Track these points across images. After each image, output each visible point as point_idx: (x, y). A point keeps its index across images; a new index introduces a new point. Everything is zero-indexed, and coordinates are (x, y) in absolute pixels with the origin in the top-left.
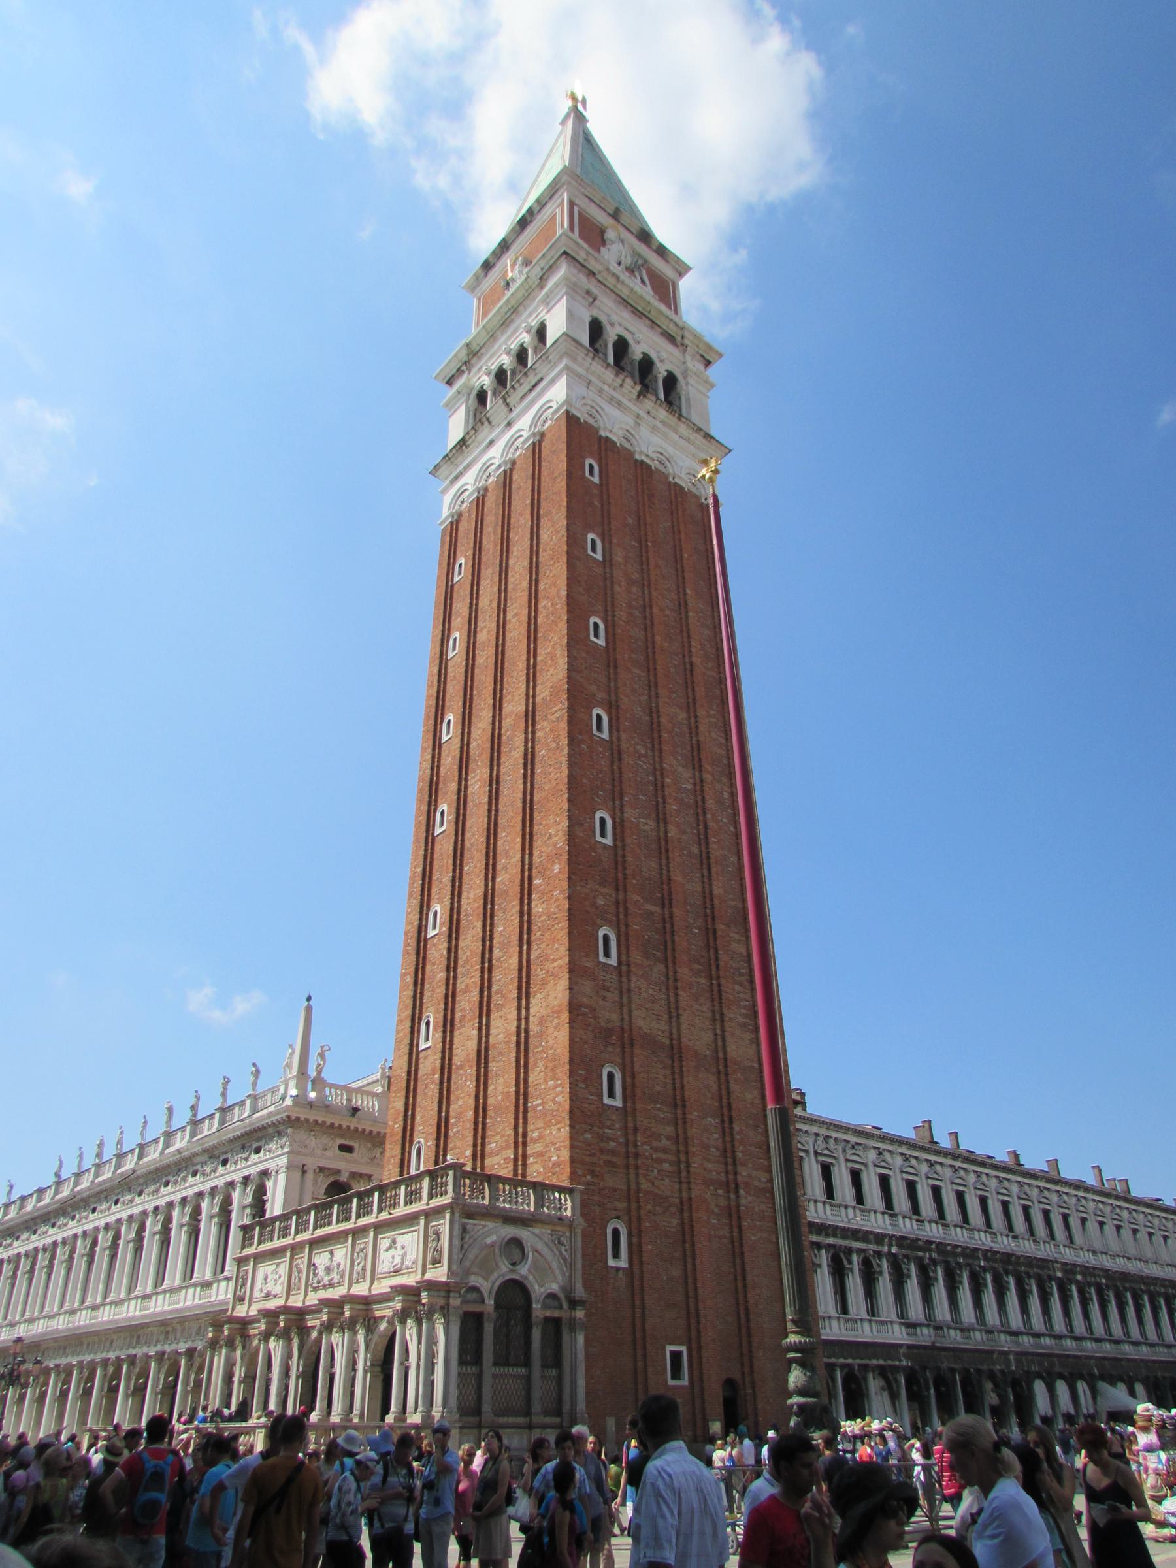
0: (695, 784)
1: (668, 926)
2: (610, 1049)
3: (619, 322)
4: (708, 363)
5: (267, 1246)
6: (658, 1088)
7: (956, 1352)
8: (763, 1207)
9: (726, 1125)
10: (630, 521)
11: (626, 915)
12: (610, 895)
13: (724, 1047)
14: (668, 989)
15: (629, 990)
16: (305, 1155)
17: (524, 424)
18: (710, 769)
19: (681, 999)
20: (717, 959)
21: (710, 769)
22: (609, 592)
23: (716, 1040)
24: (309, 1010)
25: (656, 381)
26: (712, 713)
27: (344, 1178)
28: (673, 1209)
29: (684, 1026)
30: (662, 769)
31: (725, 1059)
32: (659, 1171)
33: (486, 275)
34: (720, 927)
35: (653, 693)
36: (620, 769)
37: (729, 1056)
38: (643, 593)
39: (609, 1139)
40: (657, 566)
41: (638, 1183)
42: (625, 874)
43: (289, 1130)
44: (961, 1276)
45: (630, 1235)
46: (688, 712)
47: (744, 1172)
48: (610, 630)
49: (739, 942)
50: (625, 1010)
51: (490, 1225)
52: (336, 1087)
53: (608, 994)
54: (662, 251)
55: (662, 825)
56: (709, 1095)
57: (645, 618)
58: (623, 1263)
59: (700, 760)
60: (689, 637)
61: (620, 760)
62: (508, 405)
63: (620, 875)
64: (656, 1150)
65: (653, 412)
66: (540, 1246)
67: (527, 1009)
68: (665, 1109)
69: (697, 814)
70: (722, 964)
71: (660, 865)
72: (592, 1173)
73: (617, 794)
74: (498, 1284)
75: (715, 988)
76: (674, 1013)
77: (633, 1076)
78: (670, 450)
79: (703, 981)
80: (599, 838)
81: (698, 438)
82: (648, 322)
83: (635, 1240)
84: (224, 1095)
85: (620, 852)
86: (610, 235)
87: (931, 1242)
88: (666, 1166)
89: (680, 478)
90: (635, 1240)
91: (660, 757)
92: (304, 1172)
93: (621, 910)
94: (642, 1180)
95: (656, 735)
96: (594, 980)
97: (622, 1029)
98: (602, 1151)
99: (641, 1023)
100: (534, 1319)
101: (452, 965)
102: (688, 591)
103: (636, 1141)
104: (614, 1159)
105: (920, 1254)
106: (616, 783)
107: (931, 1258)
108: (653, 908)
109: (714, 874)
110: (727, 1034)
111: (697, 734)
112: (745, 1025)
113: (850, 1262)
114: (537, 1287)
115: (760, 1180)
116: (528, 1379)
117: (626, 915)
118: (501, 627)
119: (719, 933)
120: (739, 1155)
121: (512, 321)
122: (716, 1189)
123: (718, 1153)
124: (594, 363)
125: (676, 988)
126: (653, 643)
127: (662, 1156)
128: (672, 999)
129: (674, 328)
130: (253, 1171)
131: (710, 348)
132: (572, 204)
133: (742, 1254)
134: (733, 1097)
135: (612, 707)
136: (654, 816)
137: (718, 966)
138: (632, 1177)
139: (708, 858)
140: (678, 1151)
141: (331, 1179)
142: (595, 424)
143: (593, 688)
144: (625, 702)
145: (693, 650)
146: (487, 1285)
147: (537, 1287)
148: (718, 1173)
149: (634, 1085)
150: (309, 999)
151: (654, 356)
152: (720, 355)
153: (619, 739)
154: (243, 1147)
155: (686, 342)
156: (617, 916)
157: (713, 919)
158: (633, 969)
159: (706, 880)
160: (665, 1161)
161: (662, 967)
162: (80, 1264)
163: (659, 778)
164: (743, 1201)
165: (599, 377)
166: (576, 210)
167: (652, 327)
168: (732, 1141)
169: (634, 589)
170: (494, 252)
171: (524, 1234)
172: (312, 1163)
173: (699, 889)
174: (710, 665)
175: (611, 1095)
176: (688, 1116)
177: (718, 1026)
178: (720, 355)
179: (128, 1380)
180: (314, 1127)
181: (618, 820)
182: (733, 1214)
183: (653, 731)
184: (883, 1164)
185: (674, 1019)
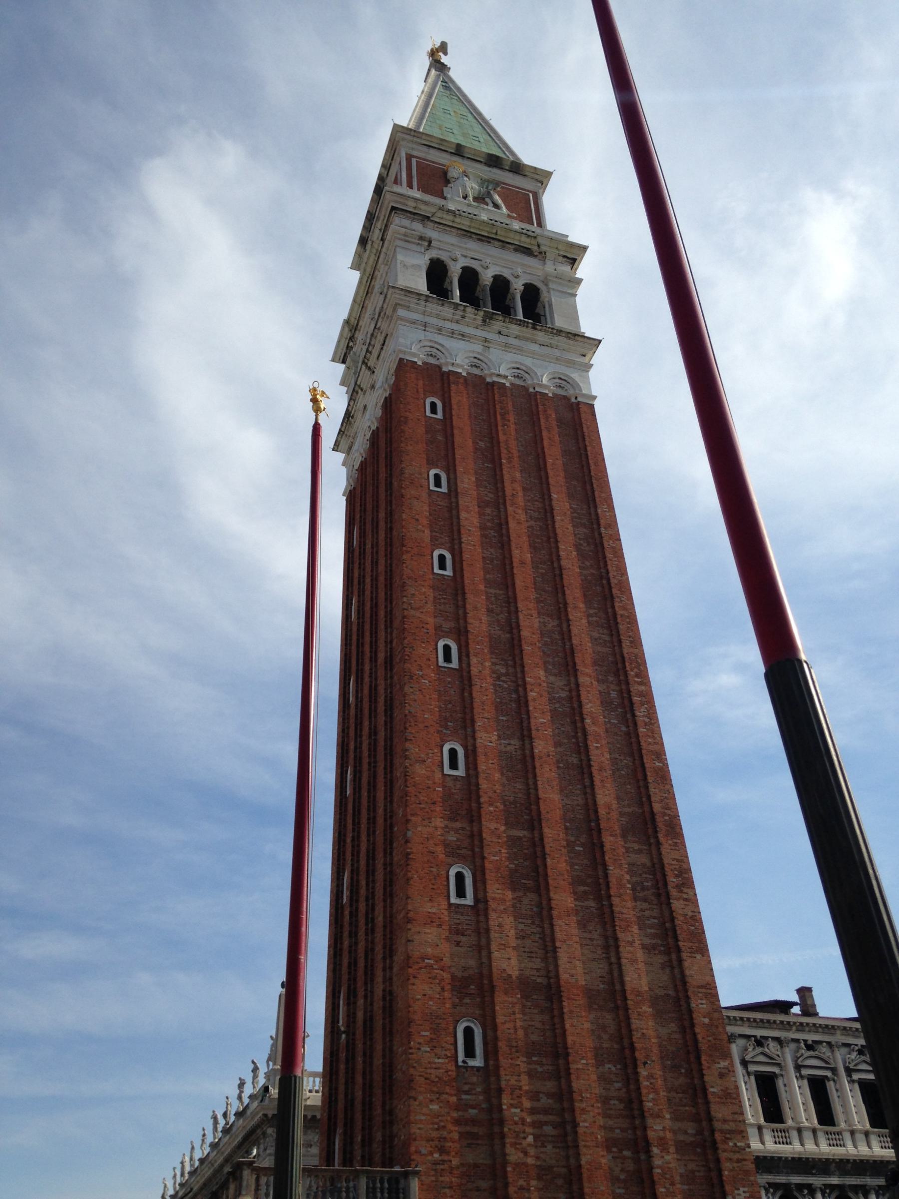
0: (570, 691)
1: (539, 849)
2: (467, 1000)
4: (573, 262)
8: (692, 1166)
10: (482, 444)
12: (463, 829)
13: (621, 975)
14: (542, 921)
15: (488, 930)
18: (587, 671)
19: (557, 929)
22: (455, 520)
23: (611, 972)
28: (560, 1182)
31: (624, 991)
32: (536, 1138)
37: (628, 987)
38: (500, 511)
40: (513, 481)
41: (505, 1155)
42: (479, 803)
46: (559, 618)
49: (639, 852)
54: (517, 168)
55: (527, 742)
56: (605, 1037)
57: (501, 536)
62: (369, 368)
65: (504, 331)
68: (544, 1060)
71: (528, 784)
72: (442, 1150)
73: (468, 722)
75: (607, 910)
77: (495, 1028)
78: (528, 362)
79: (592, 903)
80: (447, 770)
82: (497, 243)
85: (473, 781)
86: (453, 173)
93: (477, 842)
94: (509, 1150)
96: (440, 926)
97: (481, 974)
99: (504, 965)
102: (554, 496)
103: (501, 1105)
104: (475, 1130)
106: (467, 711)
108: (520, 833)
110: (624, 961)
112: (654, 947)
115: (686, 1133)
122: (621, 1151)
123: (622, 1106)
124: (428, 304)
125: (551, 918)
128: (548, 932)
129: (528, 240)
131: (572, 245)
132: (409, 158)
135: (461, 634)
136: (519, 734)
137: (608, 883)
139: (590, 766)
140: (563, 1109)
142: (437, 363)
145: (561, 553)
148: (622, 1130)
151: (506, 274)
152: (584, 249)
153: (469, 665)
155: (543, 248)
156: (473, 850)
157: (599, 831)
158: (492, 905)
159: (588, 790)
160: (546, 1123)
161: (532, 896)
164: (657, 1162)
165: (438, 316)
166: (414, 161)
167: (503, 248)
169: (488, 511)
173: (581, 802)
174: (588, 564)
176: (573, 1066)
177: (613, 954)
178: (584, 249)
181: (470, 748)
183: (511, 649)
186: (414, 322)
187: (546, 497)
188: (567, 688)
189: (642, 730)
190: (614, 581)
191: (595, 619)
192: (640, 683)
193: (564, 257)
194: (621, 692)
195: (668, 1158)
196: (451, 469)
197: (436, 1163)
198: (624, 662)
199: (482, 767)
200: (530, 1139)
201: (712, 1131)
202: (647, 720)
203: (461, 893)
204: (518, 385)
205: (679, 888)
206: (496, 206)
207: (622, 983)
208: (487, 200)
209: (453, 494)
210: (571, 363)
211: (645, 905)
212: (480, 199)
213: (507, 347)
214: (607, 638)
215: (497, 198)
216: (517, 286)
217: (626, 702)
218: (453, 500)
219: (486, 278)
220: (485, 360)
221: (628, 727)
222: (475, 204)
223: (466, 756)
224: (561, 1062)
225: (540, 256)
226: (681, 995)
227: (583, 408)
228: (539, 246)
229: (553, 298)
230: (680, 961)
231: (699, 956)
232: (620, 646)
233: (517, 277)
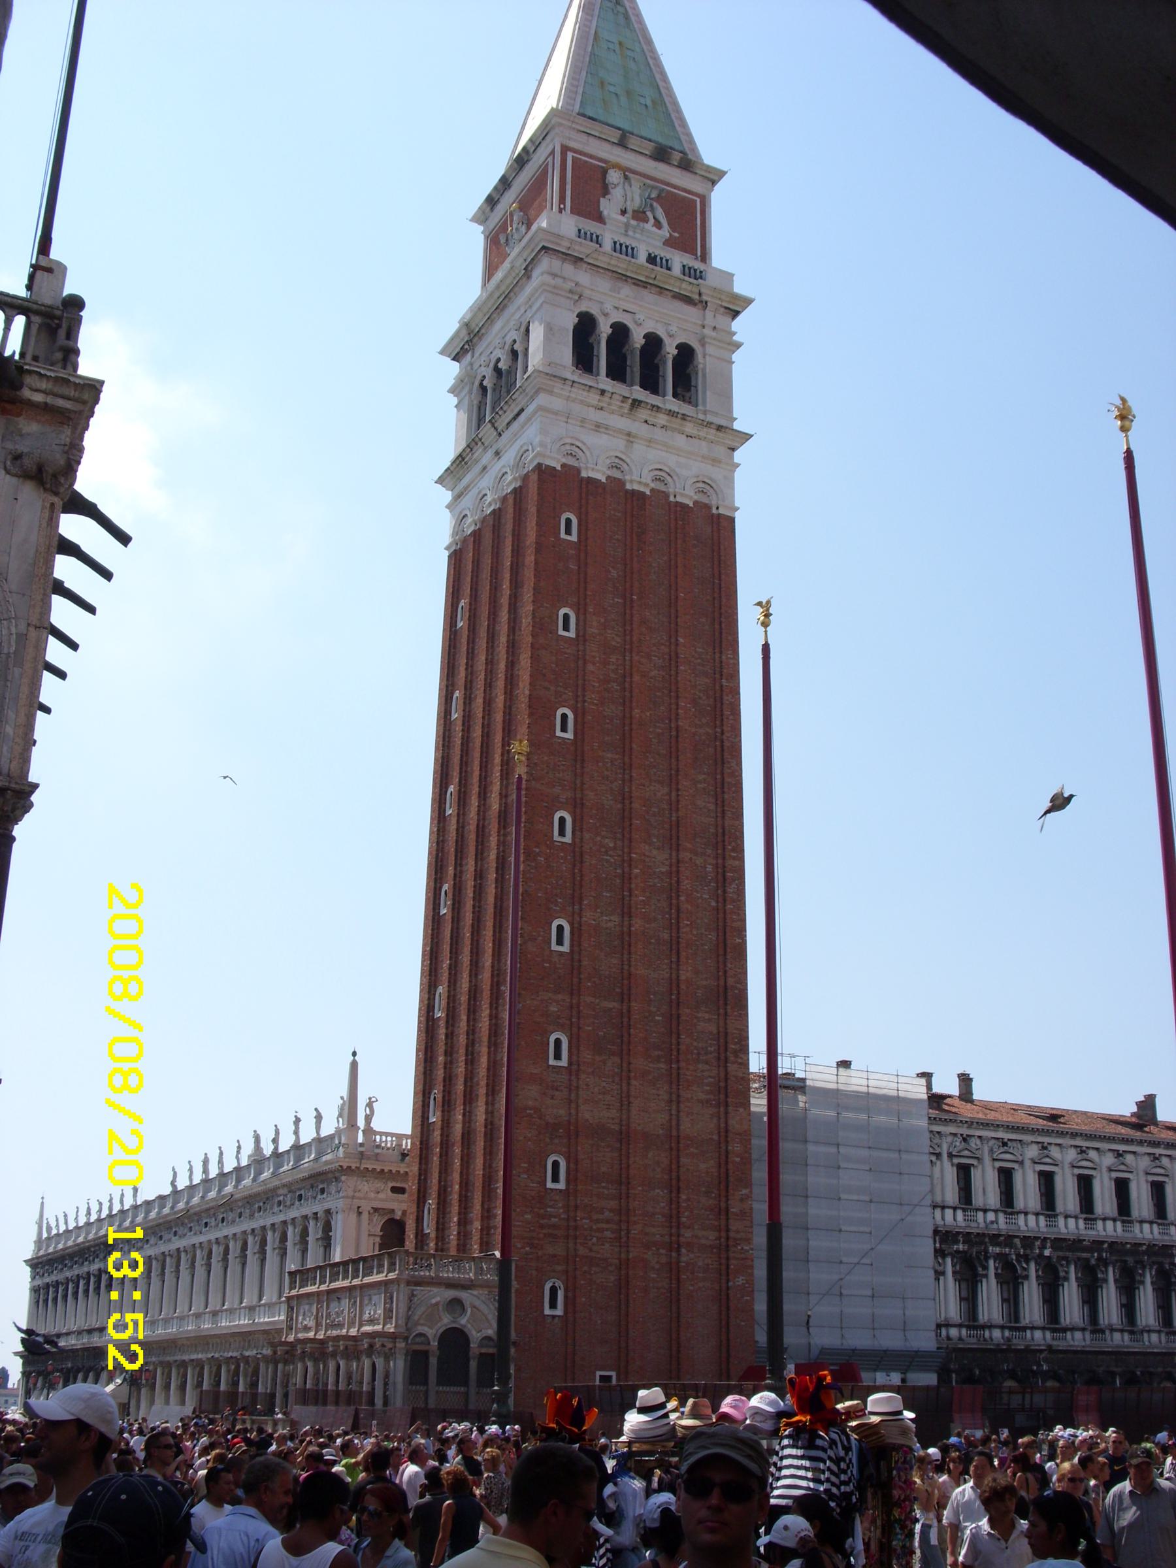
0: (671, 866)
1: (625, 1020)
2: (556, 1141)
4: (736, 314)
5: (304, 1291)
6: (604, 1169)
7: (1118, 1355)
9: (674, 1195)
11: (579, 1018)
13: (678, 1125)
15: (577, 1088)
16: (360, 1199)
17: (509, 457)
18: (688, 845)
19: (632, 1088)
20: (678, 1044)
21: (688, 845)
23: (670, 1120)
24: (354, 1066)
25: (665, 363)
26: (702, 777)
27: (398, 1215)
29: (634, 1112)
30: (631, 859)
32: (598, 1239)
33: (492, 209)
34: (685, 1011)
35: (627, 777)
36: (581, 871)
39: (551, 1216)
43: (343, 1178)
44: (1143, 1275)
45: (566, 1290)
47: (688, 1234)
48: (579, 720)
49: (710, 1020)
50: (573, 1105)
51: (435, 1290)
52: (387, 1134)
53: (557, 1093)
54: (688, 163)
57: (624, 689)
58: (559, 1312)
59: (678, 837)
60: (677, 697)
61: (582, 862)
62: (496, 429)
63: (575, 980)
64: (598, 1221)
65: (651, 420)
66: (477, 1303)
67: (493, 1104)
69: (671, 898)
70: (682, 1047)
74: (441, 1331)
75: (674, 1072)
76: (625, 1101)
77: (577, 1162)
79: (662, 1065)
80: (554, 947)
82: (654, 289)
83: (570, 1294)
84: (296, 1133)
85: (576, 957)
86: (614, 176)
87: (1103, 1242)
88: (608, 1234)
89: (682, 495)
90: (570, 1294)
91: (630, 847)
92: (360, 1213)
95: (627, 824)
97: (569, 1122)
98: (542, 1227)
99: (587, 1116)
100: (471, 1354)
101: (449, 1052)
102: (681, 640)
104: (556, 1232)
105: (1085, 1255)
107: (1100, 1259)
108: (610, 1005)
109: (683, 959)
111: (677, 810)
112: (708, 1101)
113: (986, 1268)
114: (474, 1333)
115: (707, 1239)
116: (467, 1394)
117: (579, 1018)
118: (488, 703)
119: (683, 1018)
120: (684, 1219)
121: (505, 306)
125: (629, 1078)
126: (631, 717)
127: (604, 1226)
128: (625, 1088)
130: (319, 1208)
132: (565, 149)
133: (679, 1300)
134: (682, 1170)
135: (577, 807)
138: (571, 1245)
139: (678, 942)
141: (386, 1218)
142: (576, 464)
143: (557, 790)
146: (432, 1333)
147: (474, 1333)
149: (577, 1170)
150: (354, 1054)
151: (661, 333)
154: (312, 1187)
155: (705, 298)
158: (582, 1068)
159: (674, 966)
161: (617, 1060)
162: (200, 1270)
163: (627, 870)
164: (684, 1259)
166: (570, 155)
167: (660, 294)
168: (678, 1207)
170: (496, 188)
171: (464, 1295)
172: (366, 1207)
174: (704, 721)
175: (555, 1179)
179: (245, 1376)
180: (364, 1173)
182: (674, 1270)
184: (1047, 1160)
185: (625, 1107)
186: (556, 413)
187: (673, 640)
188: (667, 863)
189: (729, 907)
190: (726, 744)
191: (702, 786)
192: (734, 858)
193: (726, 308)
194: (716, 866)
195: (692, 1256)
196: (580, 609)
197: (527, 1254)
198: (724, 834)
199: (585, 945)
200: (594, 1239)
201: (728, 1239)
202: (735, 896)
203: (558, 1056)
204: (659, 491)
205: (736, 1053)
207: (678, 1130)
208: (649, 214)
209: (581, 638)
210: (715, 461)
211: (707, 1067)
212: (640, 215)
213: (650, 442)
214: (712, 807)
215: (660, 214)
216: (670, 350)
217: (720, 877)
218: (581, 648)
220: (628, 460)
221: (717, 902)
222: (634, 223)
223: (572, 933)
224: (623, 1187)
225: (700, 306)
226: (722, 1139)
228: (700, 294)
229: (705, 361)
230: (726, 1113)
231: (741, 1110)
232: (723, 817)
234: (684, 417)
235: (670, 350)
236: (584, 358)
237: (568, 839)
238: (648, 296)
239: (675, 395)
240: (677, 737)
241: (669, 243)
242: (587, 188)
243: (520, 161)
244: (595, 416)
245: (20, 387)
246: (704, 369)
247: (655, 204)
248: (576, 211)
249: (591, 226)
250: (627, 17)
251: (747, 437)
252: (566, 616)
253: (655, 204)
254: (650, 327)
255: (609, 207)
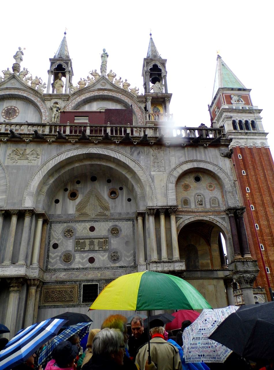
3: (238, 117)
25: (249, 125)
30: (266, 211)
54: (244, 90)
60: (267, 181)
81: (262, 135)
86: (232, 96)
108: (270, 238)
132: (223, 94)
135: (254, 203)
144: (256, 202)
145: (269, 184)
166: (224, 95)
196: (246, 170)
206: (242, 101)
212: (238, 101)
215: (242, 99)
216: (250, 122)
219: (244, 122)
222: (238, 103)
223: (259, 226)
227: (268, 149)
229: (257, 123)
233: (249, 120)
234: (256, 133)
235: (250, 122)
236: (235, 128)
237: (254, 209)
238: (244, 115)
239: (253, 130)
240: (269, 188)
241: (245, 104)
242: (229, 99)
243: (215, 98)
244: (240, 137)
245: (220, 142)
246: (257, 124)
247: (241, 98)
248: (228, 104)
249: (230, 105)
250: (227, 69)
251: (268, 133)
252: (243, 172)
253: (241, 98)
254: (245, 119)
255: (232, 101)
